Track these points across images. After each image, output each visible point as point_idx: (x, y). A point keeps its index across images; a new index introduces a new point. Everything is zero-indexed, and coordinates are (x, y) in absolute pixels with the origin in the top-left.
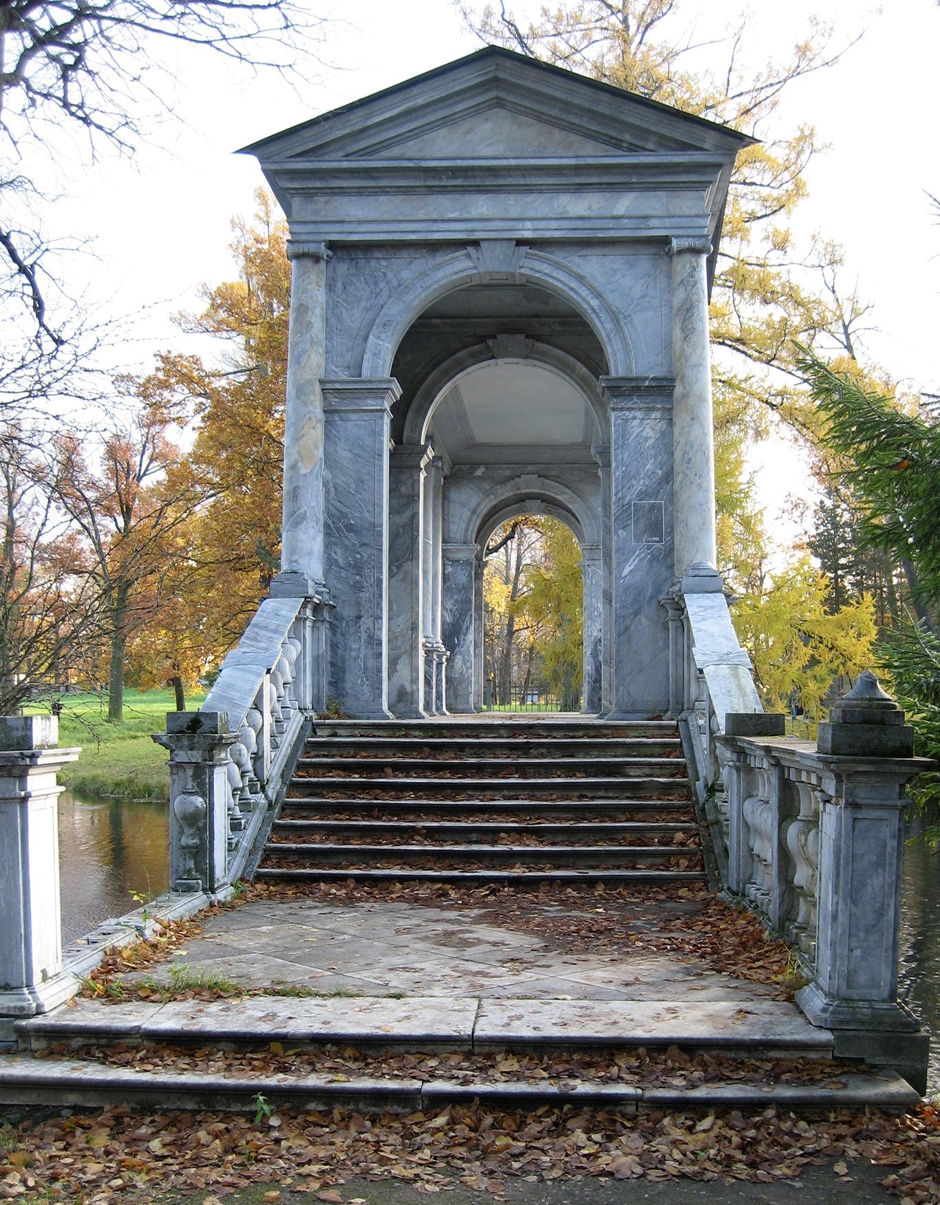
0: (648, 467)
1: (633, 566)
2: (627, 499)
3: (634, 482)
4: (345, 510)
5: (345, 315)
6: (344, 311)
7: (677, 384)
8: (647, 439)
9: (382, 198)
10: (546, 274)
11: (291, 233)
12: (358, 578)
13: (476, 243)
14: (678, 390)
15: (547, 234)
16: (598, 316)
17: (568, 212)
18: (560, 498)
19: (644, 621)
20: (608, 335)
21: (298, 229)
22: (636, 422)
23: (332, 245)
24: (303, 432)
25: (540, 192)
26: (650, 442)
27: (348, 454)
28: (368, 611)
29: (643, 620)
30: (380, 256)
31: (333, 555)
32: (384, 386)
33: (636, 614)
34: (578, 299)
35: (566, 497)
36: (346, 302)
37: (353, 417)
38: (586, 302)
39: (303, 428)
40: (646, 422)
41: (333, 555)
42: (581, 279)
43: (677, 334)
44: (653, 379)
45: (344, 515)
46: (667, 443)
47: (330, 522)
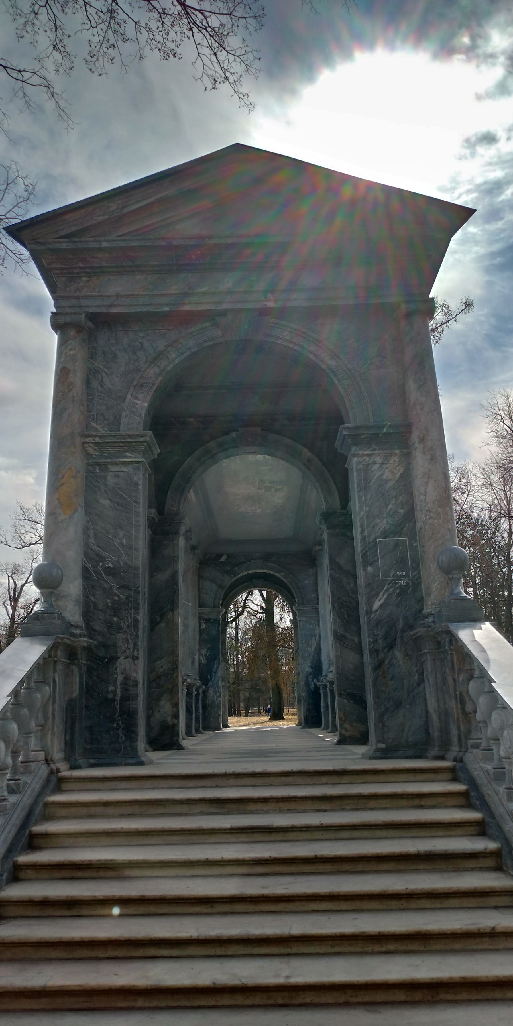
0: (390, 507)
1: (382, 601)
2: (373, 537)
4: (104, 554)
5: (106, 380)
6: (104, 375)
8: (387, 481)
10: (287, 340)
11: (55, 306)
12: (115, 619)
14: (415, 436)
21: (63, 303)
22: (376, 467)
23: (92, 317)
26: (390, 484)
27: (107, 503)
28: (124, 652)
29: (398, 654)
31: (92, 598)
32: (141, 439)
33: (391, 646)
35: (283, 574)
36: (108, 368)
37: (114, 469)
39: (63, 477)
40: (385, 466)
41: (92, 598)
44: (390, 426)
45: (103, 559)
47: (89, 566)
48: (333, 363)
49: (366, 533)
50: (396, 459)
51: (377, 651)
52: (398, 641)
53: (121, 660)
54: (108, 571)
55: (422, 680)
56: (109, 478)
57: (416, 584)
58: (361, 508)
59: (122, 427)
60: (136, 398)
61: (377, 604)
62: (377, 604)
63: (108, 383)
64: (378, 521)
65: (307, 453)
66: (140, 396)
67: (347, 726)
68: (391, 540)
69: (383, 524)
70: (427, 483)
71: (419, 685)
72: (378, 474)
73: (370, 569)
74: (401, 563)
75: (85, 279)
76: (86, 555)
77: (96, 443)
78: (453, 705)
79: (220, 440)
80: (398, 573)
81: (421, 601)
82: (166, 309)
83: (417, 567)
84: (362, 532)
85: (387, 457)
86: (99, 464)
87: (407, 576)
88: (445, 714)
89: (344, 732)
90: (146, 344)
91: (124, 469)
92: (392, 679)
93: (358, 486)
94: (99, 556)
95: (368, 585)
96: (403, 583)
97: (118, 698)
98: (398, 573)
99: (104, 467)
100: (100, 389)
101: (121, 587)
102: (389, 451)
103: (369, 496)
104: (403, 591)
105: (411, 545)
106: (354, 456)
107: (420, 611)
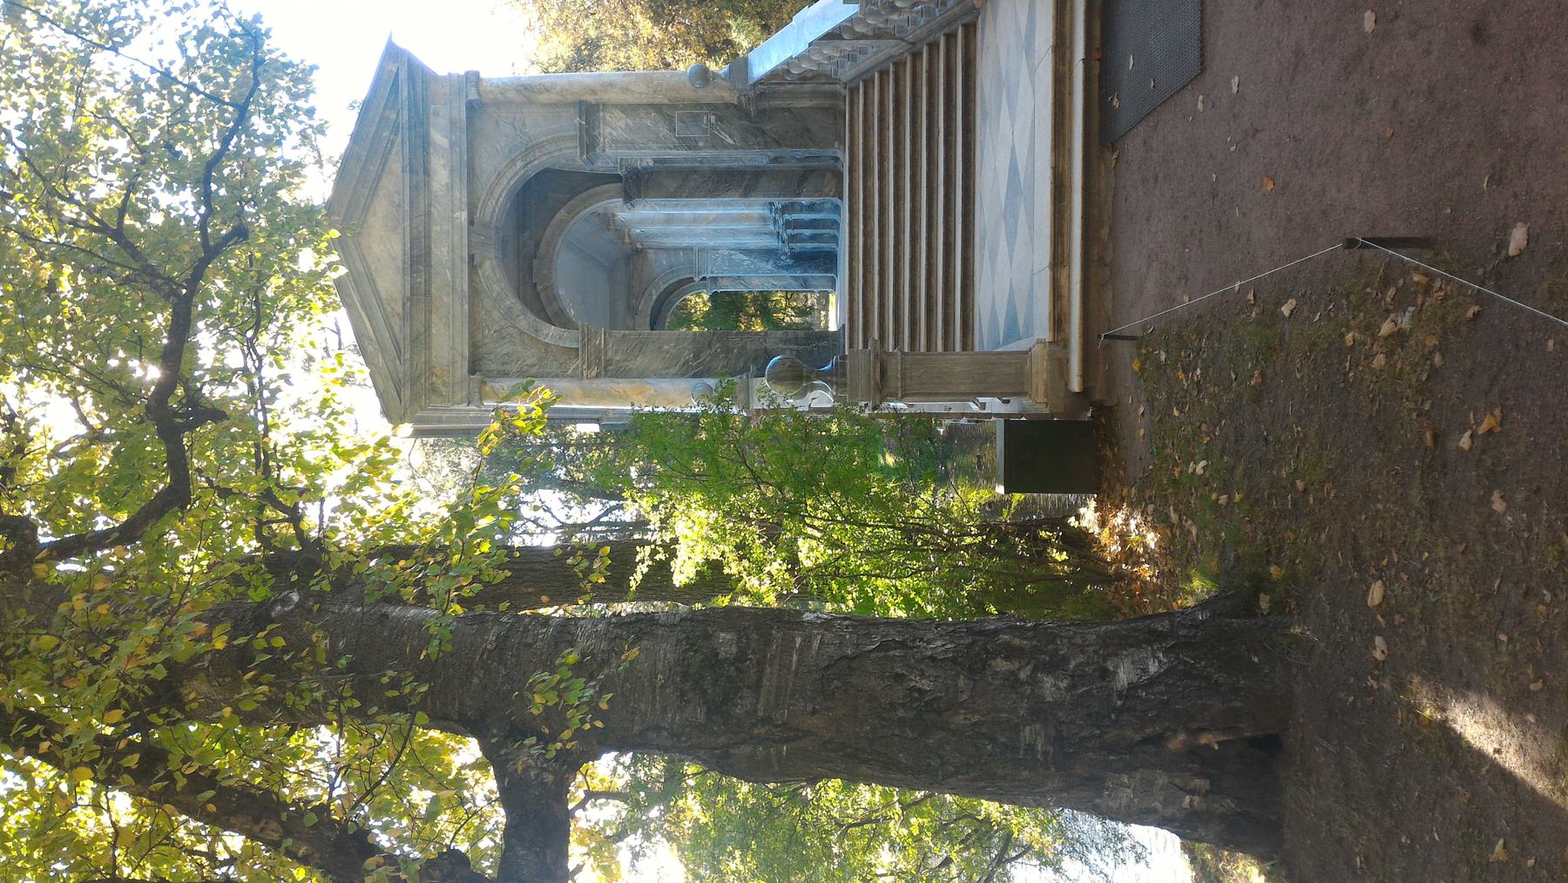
3: (661, 135)
4: (682, 360)
5: (528, 362)
7: (583, 98)
8: (627, 125)
9: (434, 331)
13: (471, 257)
14: (590, 98)
15: (465, 199)
16: (530, 162)
17: (447, 184)
18: (654, 297)
19: (768, 128)
20: (545, 154)
22: (614, 133)
23: (472, 371)
24: (621, 392)
25: (430, 205)
26: (629, 122)
30: (480, 335)
33: (763, 133)
34: (516, 178)
35: (654, 291)
37: (610, 354)
38: (518, 172)
42: (499, 175)
43: (544, 98)
46: (628, 109)
47: (692, 373)
48: (519, 164)
49: (671, 146)
50: (608, 116)
51: (766, 143)
52: (759, 126)
53: (768, 346)
54: (696, 357)
55: (789, 110)
56: (618, 358)
57: (713, 107)
58: (650, 148)
59: (574, 346)
60: (547, 335)
61: (730, 141)
62: (730, 141)
63: (533, 360)
64: (661, 135)
65: (562, 214)
66: (545, 332)
67: (827, 189)
68: (677, 125)
69: (663, 130)
70: (632, 91)
71: (792, 113)
72: (621, 132)
73: (701, 144)
74: (696, 118)
75: (434, 379)
76: (682, 376)
77: (588, 368)
78: (807, 87)
79: (544, 301)
80: (705, 121)
81: (728, 105)
82: (466, 307)
83: (700, 106)
84: (670, 149)
85: (605, 123)
86: (605, 368)
87: (706, 114)
88: (814, 94)
89: (831, 194)
90: (496, 327)
91: (610, 346)
92: (787, 133)
93: (630, 149)
94: (684, 365)
95: (714, 147)
96: (713, 118)
97: (796, 347)
98: (705, 121)
99: (609, 362)
100: (537, 367)
101: (710, 346)
102: (601, 121)
103: (640, 141)
104: (719, 119)
105: (682, 109)
106: (604, 151)
107: (736, 106)
